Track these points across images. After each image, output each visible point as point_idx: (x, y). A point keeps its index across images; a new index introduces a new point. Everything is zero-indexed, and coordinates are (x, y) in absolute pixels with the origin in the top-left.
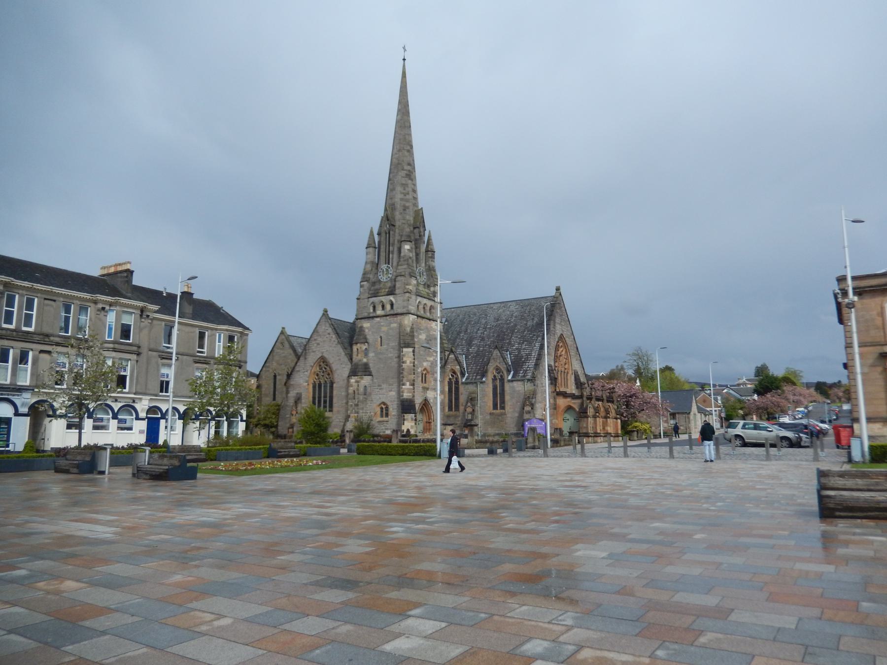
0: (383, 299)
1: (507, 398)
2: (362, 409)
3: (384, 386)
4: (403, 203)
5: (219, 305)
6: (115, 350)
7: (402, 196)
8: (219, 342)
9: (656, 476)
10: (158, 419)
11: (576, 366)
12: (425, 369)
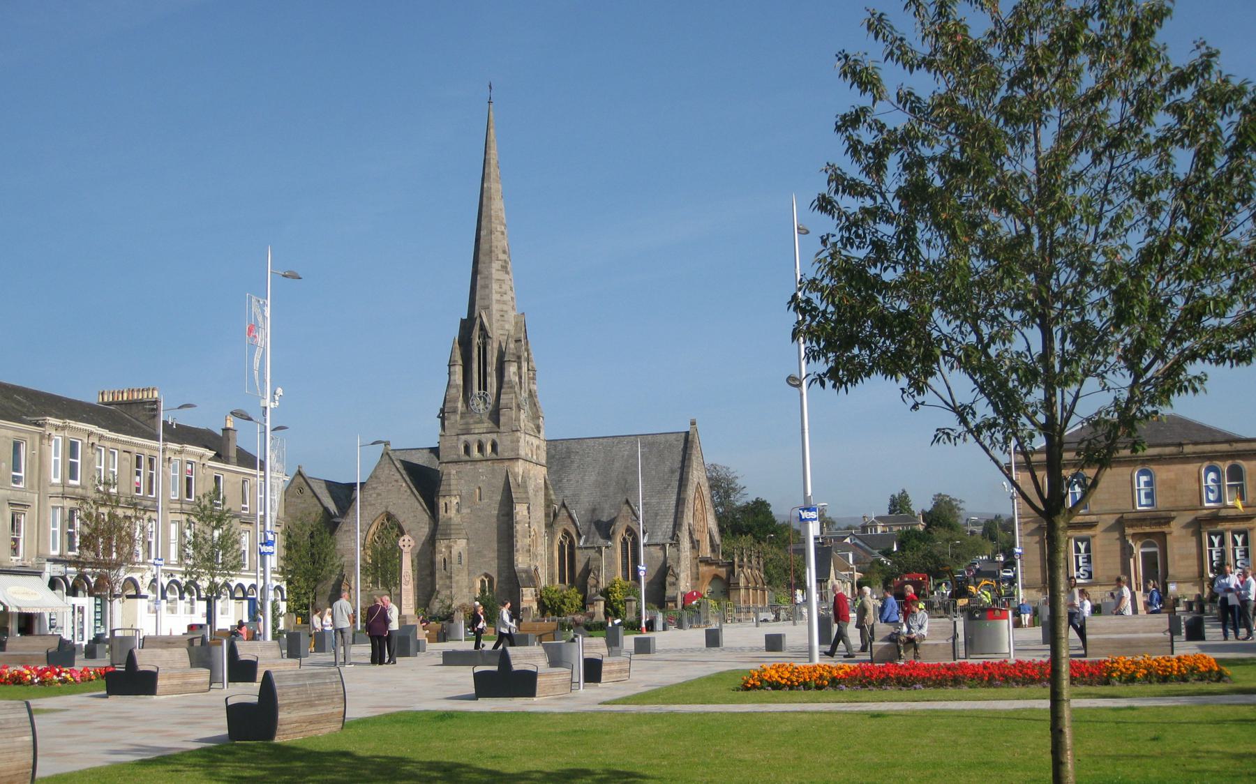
5: (203, 426)
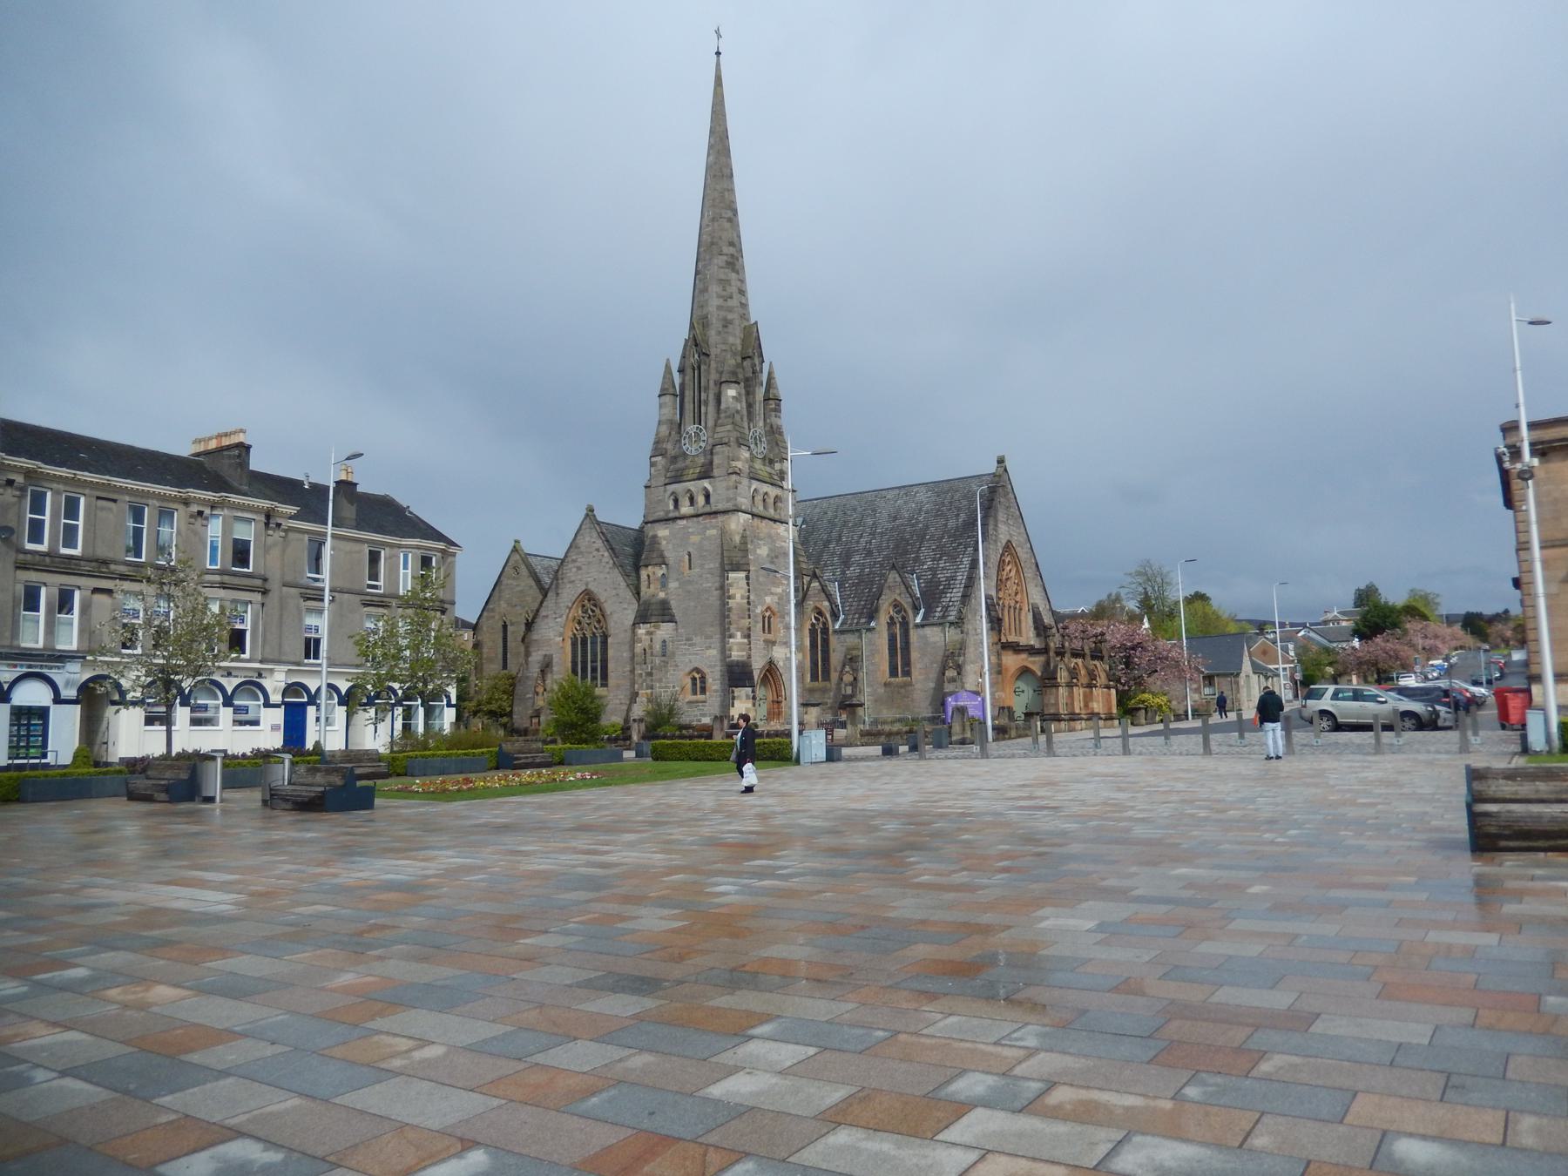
0: (691, 485)
1: (914, 655)
2: (660, 681)
3: (697, 640)
4: (722, 313)
6: (224, 586)
7: (720, 302)
8: (405, 567)
9: (1180, 786)
10: (303, 706)
11: (1036, 597)
12: (769, 608)
